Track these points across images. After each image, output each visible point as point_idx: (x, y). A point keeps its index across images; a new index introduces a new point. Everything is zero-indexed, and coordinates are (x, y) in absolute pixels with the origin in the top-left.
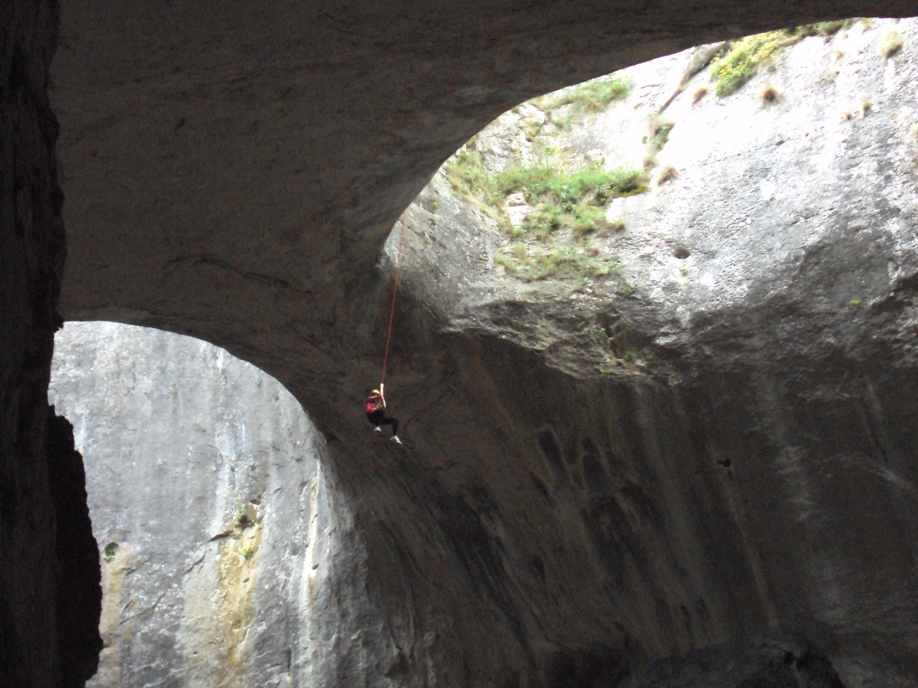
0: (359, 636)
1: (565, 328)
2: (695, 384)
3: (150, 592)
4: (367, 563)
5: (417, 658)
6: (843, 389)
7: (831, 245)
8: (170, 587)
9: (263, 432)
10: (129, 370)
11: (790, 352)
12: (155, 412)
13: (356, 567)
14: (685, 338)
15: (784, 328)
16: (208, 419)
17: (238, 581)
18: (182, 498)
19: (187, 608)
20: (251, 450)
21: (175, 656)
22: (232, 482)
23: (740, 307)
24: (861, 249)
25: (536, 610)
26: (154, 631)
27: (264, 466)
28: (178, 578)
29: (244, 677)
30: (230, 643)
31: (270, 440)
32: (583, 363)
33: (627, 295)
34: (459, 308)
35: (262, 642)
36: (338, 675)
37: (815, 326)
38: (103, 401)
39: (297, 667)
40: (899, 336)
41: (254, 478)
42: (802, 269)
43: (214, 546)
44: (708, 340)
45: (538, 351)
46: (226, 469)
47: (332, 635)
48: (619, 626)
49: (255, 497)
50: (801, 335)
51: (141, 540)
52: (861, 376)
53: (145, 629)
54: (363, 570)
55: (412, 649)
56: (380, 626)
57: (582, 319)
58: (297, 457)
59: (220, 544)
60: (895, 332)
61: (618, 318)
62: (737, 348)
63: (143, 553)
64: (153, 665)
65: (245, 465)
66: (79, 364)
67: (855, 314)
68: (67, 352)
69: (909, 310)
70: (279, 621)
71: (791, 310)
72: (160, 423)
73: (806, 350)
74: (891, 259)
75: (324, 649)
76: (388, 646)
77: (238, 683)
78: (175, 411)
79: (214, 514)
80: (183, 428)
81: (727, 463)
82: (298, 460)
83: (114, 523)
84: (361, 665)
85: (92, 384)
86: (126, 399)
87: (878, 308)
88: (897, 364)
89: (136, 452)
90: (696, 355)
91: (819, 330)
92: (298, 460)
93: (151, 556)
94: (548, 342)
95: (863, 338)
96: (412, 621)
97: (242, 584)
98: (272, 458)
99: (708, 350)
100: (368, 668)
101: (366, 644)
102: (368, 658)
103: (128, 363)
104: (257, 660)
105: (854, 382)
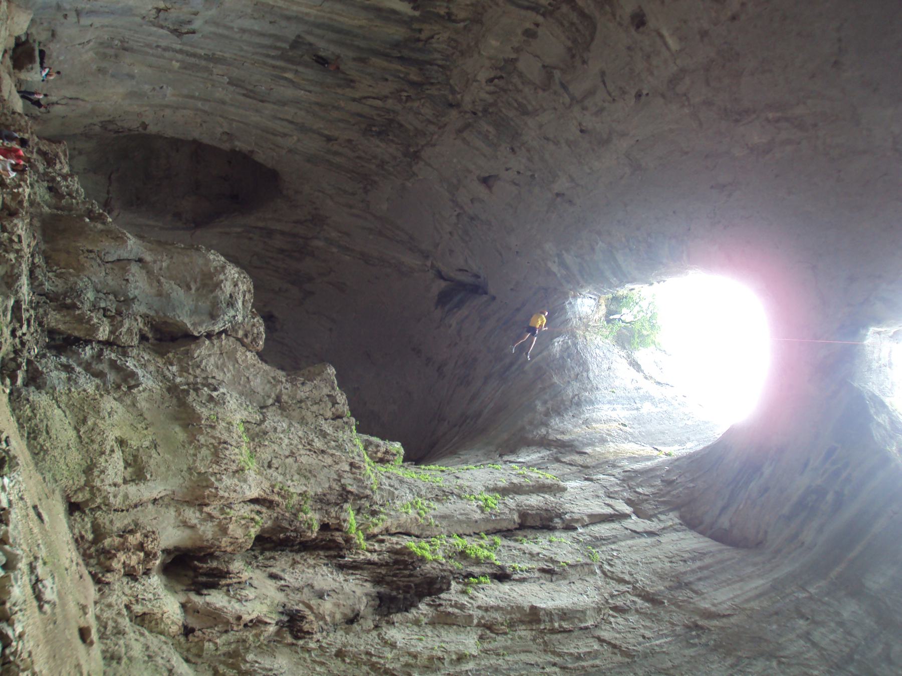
25: (741, 507)
28: (630, 441)
35: (635, 457)
45: (873, 418)
48: (766, 532)
53: (605, 436)
93: (631, 434)
94: (880, 420)
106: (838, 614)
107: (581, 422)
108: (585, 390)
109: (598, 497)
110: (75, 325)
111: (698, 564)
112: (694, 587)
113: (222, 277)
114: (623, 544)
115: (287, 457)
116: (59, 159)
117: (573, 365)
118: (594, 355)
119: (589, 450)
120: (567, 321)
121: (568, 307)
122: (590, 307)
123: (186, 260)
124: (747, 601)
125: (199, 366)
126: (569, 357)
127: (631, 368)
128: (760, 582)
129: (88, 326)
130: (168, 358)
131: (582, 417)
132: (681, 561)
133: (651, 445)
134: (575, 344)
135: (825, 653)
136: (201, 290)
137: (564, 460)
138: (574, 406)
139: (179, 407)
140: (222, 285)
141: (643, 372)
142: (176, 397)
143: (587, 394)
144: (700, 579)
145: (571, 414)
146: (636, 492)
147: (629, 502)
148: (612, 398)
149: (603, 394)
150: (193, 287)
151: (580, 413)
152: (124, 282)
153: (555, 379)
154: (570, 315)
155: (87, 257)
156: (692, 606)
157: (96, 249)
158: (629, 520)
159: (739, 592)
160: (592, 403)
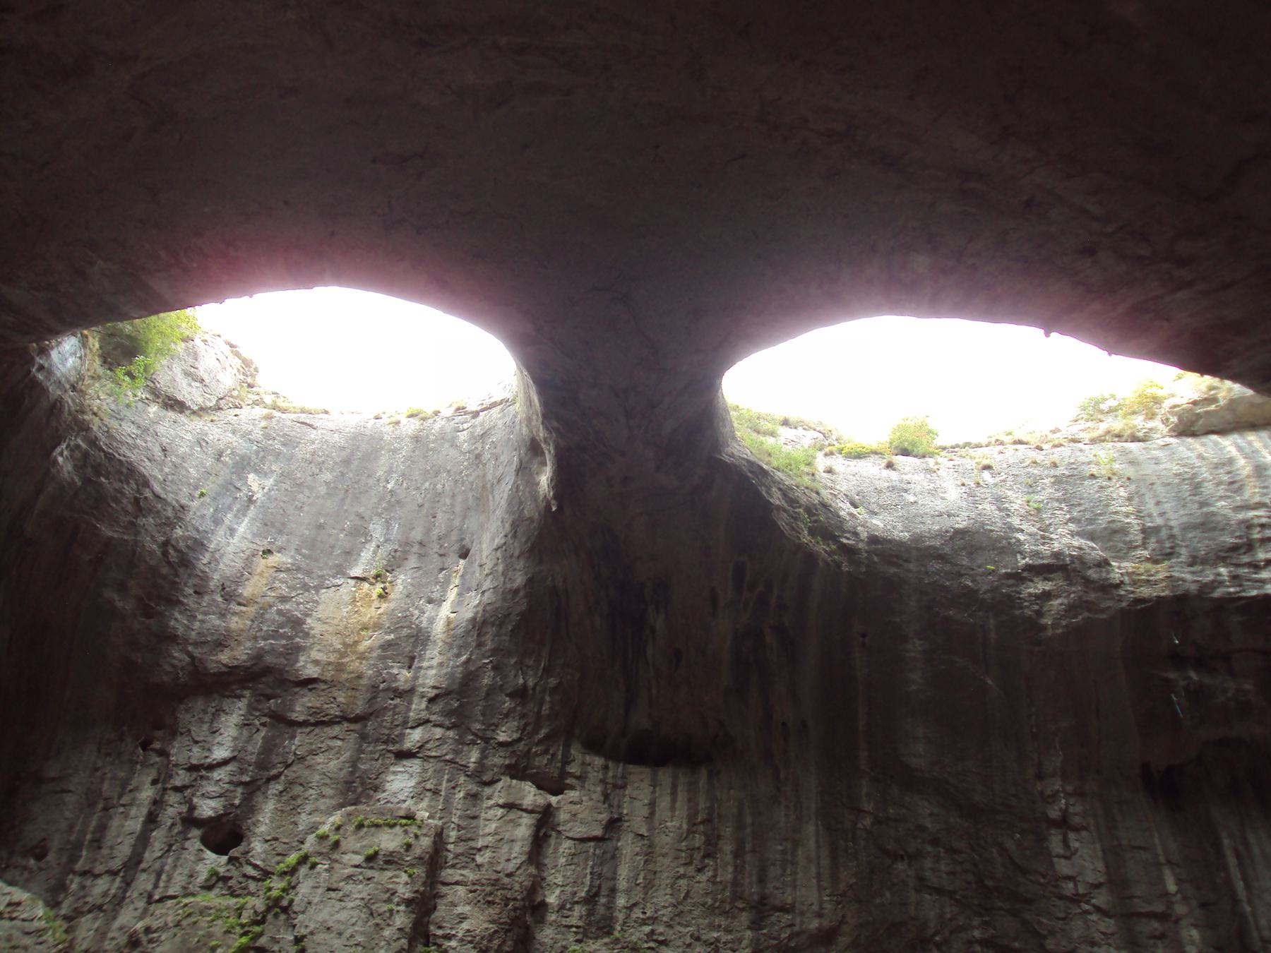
0: (491, 662)
1: (786, 502)
2: (861, 576)
3: (293, 588)
4: (522, 614)
5: (537, 692)
6: (969, 616)
7: (974, 533)
8: (309, 591)
9: (413, 532)
10: (319, 464)
11: (935, 581)
12: (327, 494)
13: (509, 614)
14: (861, 545)
15: (935, 566)
16: (369, 512)
17: (370, 606)
18: (333, 547)
19: (320, 607)
20: (399, 541)
21: (302, 631)
22: (375, 553)
23: (905, 543)
24: (995, 541)
25: (654, 691)
26: (289, 611)
27: (405, 552)
28: (317, 589)
29: (364, 662)
30: (356, 639)
31: (419, 538)
32: (793, 529)
33: (825, 506)
34: (729, 450)
36: (460, 683)
37: (959, 572)
38: (293, 471)
39: (421, 668)
40: (1021, 596)
41: (393, 557)
42: (951, 538)
43: (352, 582)
44: (876, 553)
46: (374, 544)
47: (462, 655)
49: (389, 569)
50: (947, 573)
51: (292, 557)
52: (987, 612)
53: (282, 607)
54: (514, 618)
55: (536, 685)
56: (513, 661)
57: (798, 503)
58: (442, 552)
59: (357, 583)
60: (1020, 594)
61: (818, 515)
62: (898, 566)
63: (293, 565)
64: (281, 630)
65: (389, 547)
66: (284, 445)
67: (989, 574)
68: (278, 435)
69: (1031, 584)
70: (409, 636)
71: (941, 557)
72: (329, 502)
73: (948, 583)
74: (1020, 553)
75: (452, 663)
76: (516, 676)
77: (357, 664)
78: (343, 499)
79: (357, 565)
80: (346, 510)
81: (864, 636)
82: (441, 555)
83: (275, 539)
84: (486, 681)
85: (291, 458)
86: (309, 478)
87: (1008, 576)
88: (1017, 612)
89: (306, 509)
90: (867, 558)
91: (961, 575)
92: (441, 555)
95: (995, 590)
96: (542, 665)
97: (373, 609)
98: (416, 549)
99: (876, 559)
100: (492, 685)
101: (494, 668)
102: (494, 678)
103: (320, 460)
104: (379, 655)
105: (981, 614)
106: (922, 828)
107: (220, 599)
108: (169, 524)
109: (474, 797)
111: (727, 848)
112: (777, 902)
114: (622, 884)
117: (117, 485)
118: (130, 441)
119: (311, 671)
120: (56, 407)
121: (40, 376)
122: (75, 353)
124: (834, 876)
126: (98, 474)
127: (172, 415)
128: (810, 829)
131: (211, 584)
132: (705, 857)
133: (340, 571)
134: (93, 442)
135: (958, 897)
137: (298, 714)
138: (181, 570)
141: (189, 408)
143: (179, 532)
144: (762, 881)
145: (191, 591)
146: (501, 744)
147: (517, 771)
148: (212, 510)
149: (199, 512)
151: (202, 579)
153: (107, 531)
154: (54, 391)
156: (804, 937)
158: (563, 816)
159: (813, 870)
160: (199, 545)
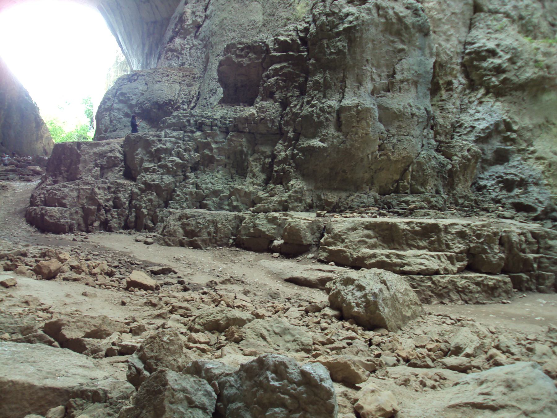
110: (469, 172)
113: (391, 12)
115: (544, 7)
116: (106, 152)
123: (370, 45)
125: (451, 58)
129: (473, 161)
130: (442, 84)
136: (403, 38)
139: (524, 90)
140: (401, 14)
142: (511, 90)
150: (401, 46)
152: (415, 119)
155: (393, 152)
157: (379, 142)
